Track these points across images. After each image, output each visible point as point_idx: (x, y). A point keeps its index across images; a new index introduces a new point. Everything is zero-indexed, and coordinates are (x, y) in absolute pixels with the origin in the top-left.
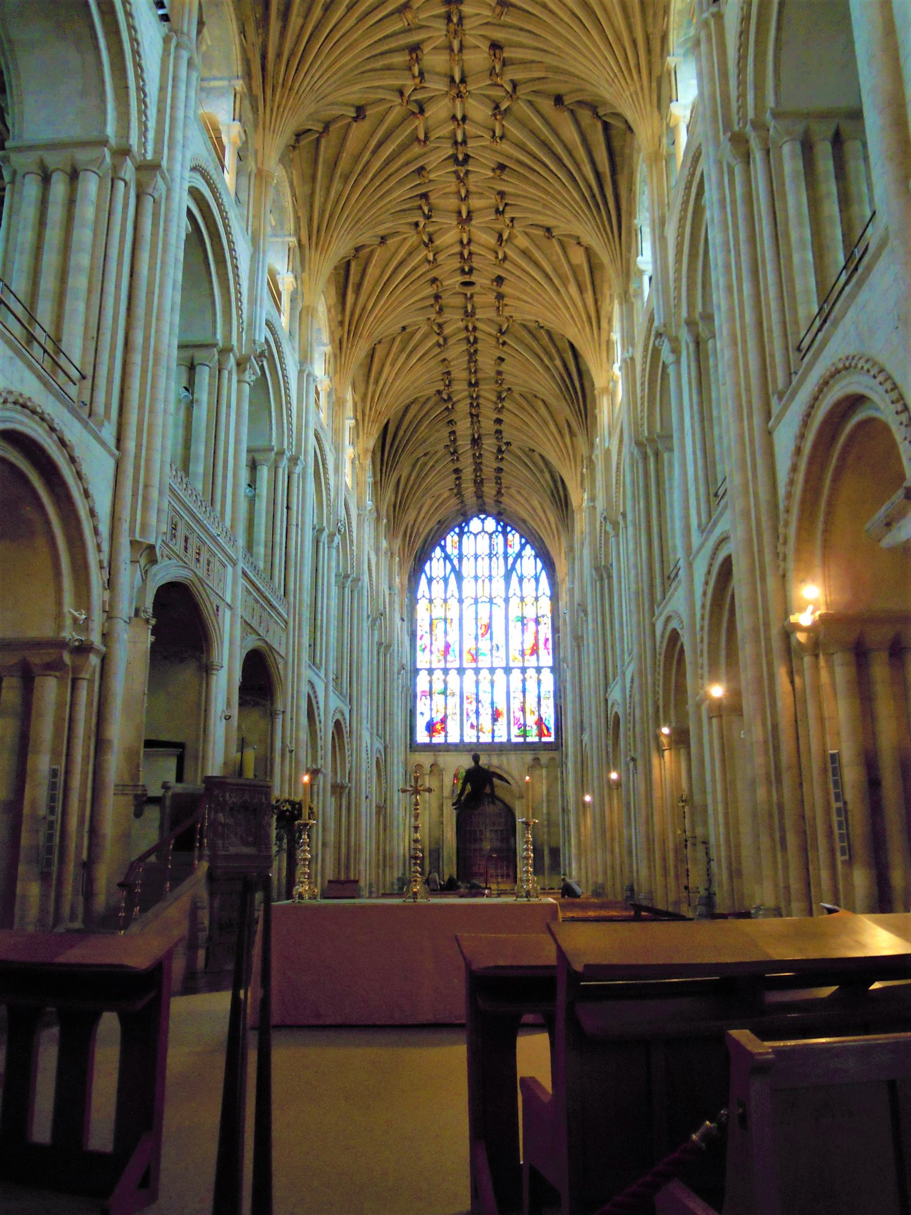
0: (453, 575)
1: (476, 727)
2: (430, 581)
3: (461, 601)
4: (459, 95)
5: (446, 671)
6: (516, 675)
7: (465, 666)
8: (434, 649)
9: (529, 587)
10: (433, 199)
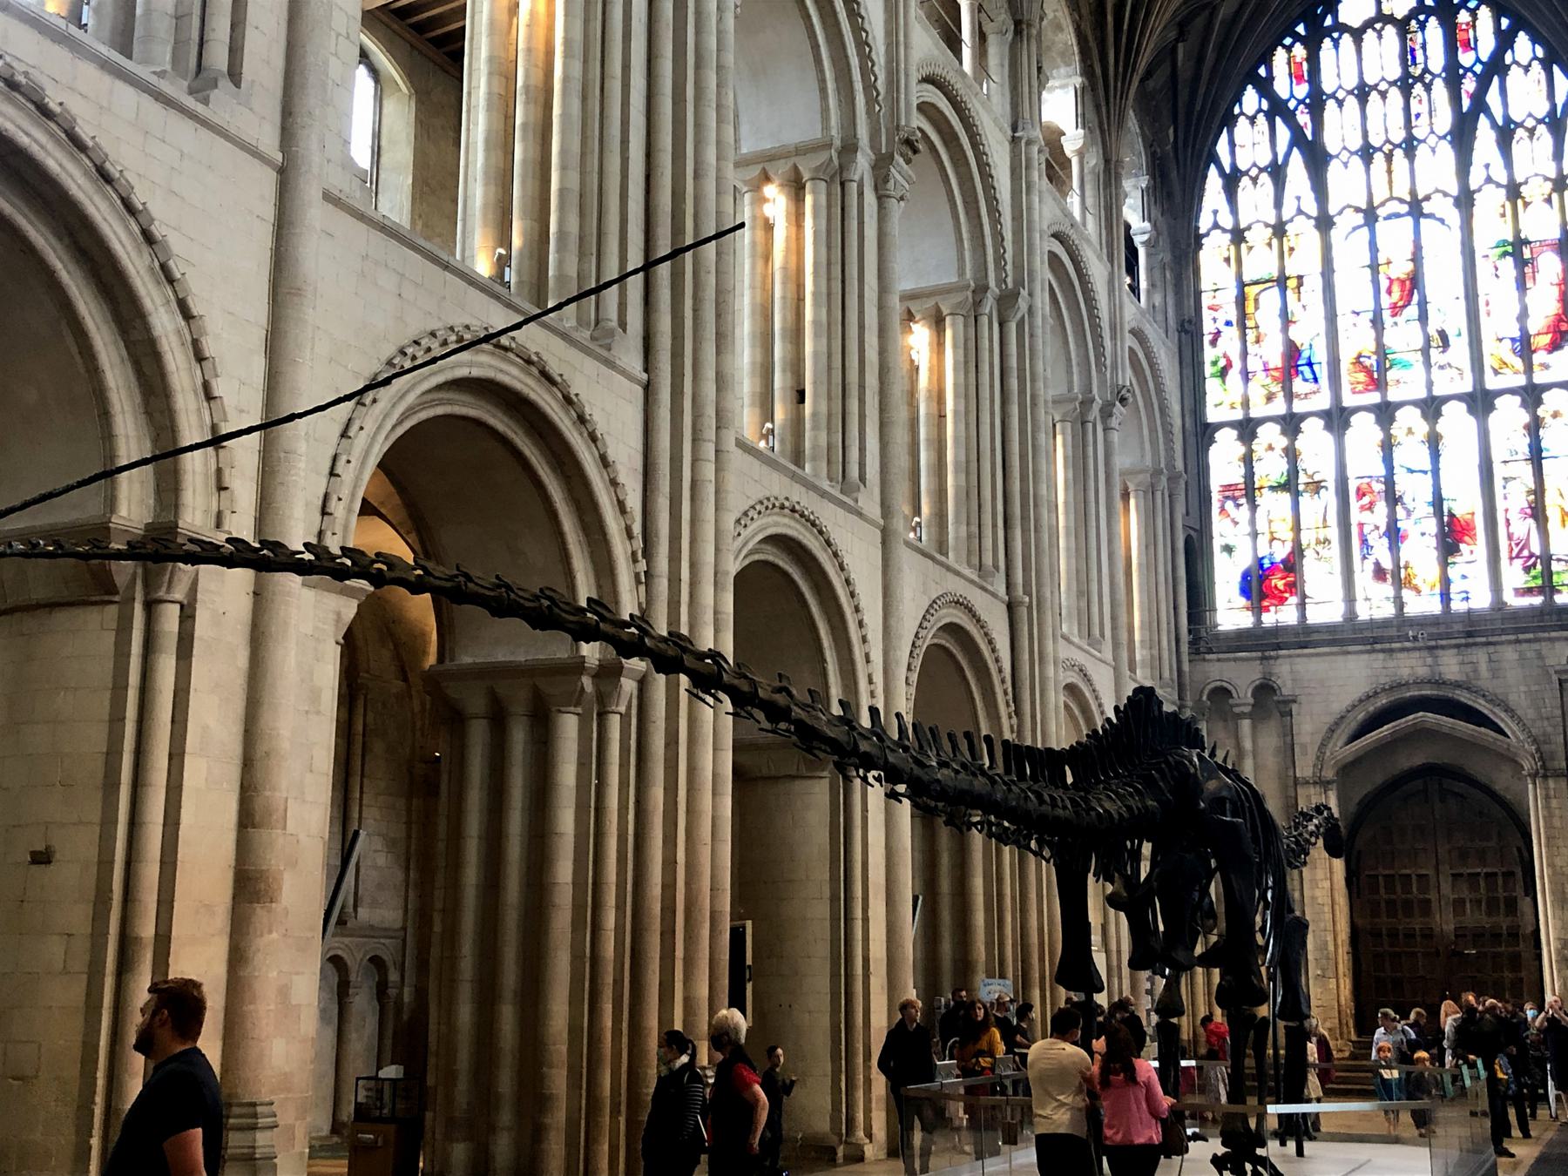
0: (1297, 157)
1: (1397, 577)
2: (1231, 181)
3: (1324, 223)
7: (1349, 400)
8: (1254, 364)
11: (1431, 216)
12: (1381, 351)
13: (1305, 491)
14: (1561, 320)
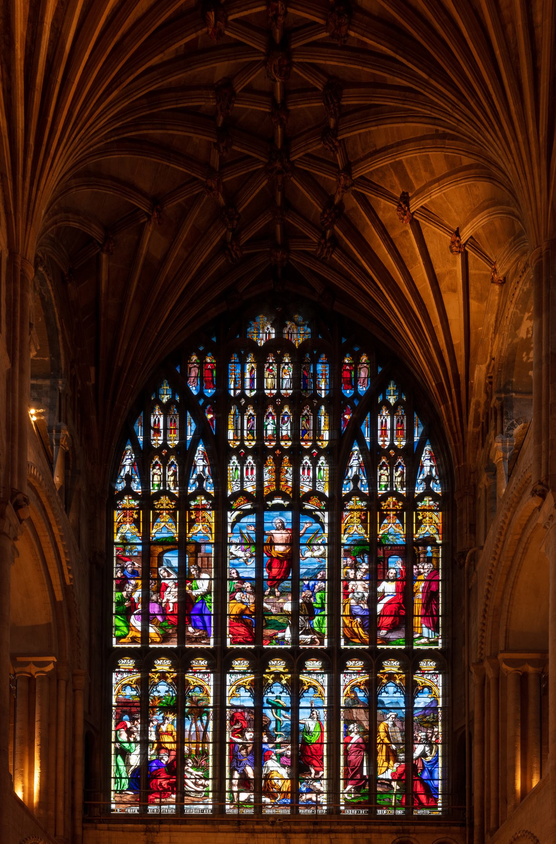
11: (309, 513)
12: (260, 611)
13: (189, 713)
14: (400, 608)
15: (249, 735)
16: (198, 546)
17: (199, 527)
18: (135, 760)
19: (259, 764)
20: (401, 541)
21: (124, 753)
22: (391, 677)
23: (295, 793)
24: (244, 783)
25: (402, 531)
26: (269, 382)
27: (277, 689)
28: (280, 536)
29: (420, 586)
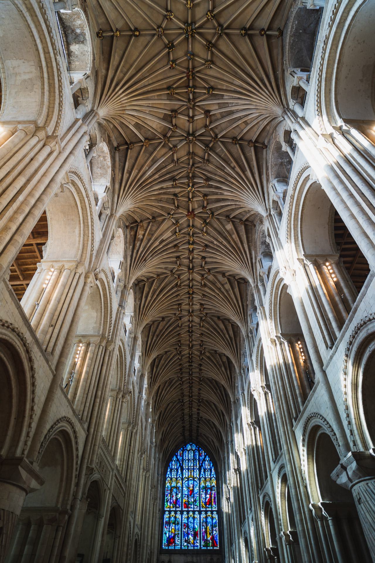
4: (191, 316)
5: (176, 512)
6: (203, 515)
9: (208, 474)
10: (182, 342)
12: (188, 501)
15: (186, 529)
16: (179, 487)
17: (179, 484)
18: (167, 535)
19: (188, 537)
20: (210, 487)
21: (166, 534)
22: (209, 516)
23: (194, 543)
24: (186, 541)
25: (210, 485)
26: (190, 456)
27: (191, 518)
28: (191, 486)
29: (213, 496)
